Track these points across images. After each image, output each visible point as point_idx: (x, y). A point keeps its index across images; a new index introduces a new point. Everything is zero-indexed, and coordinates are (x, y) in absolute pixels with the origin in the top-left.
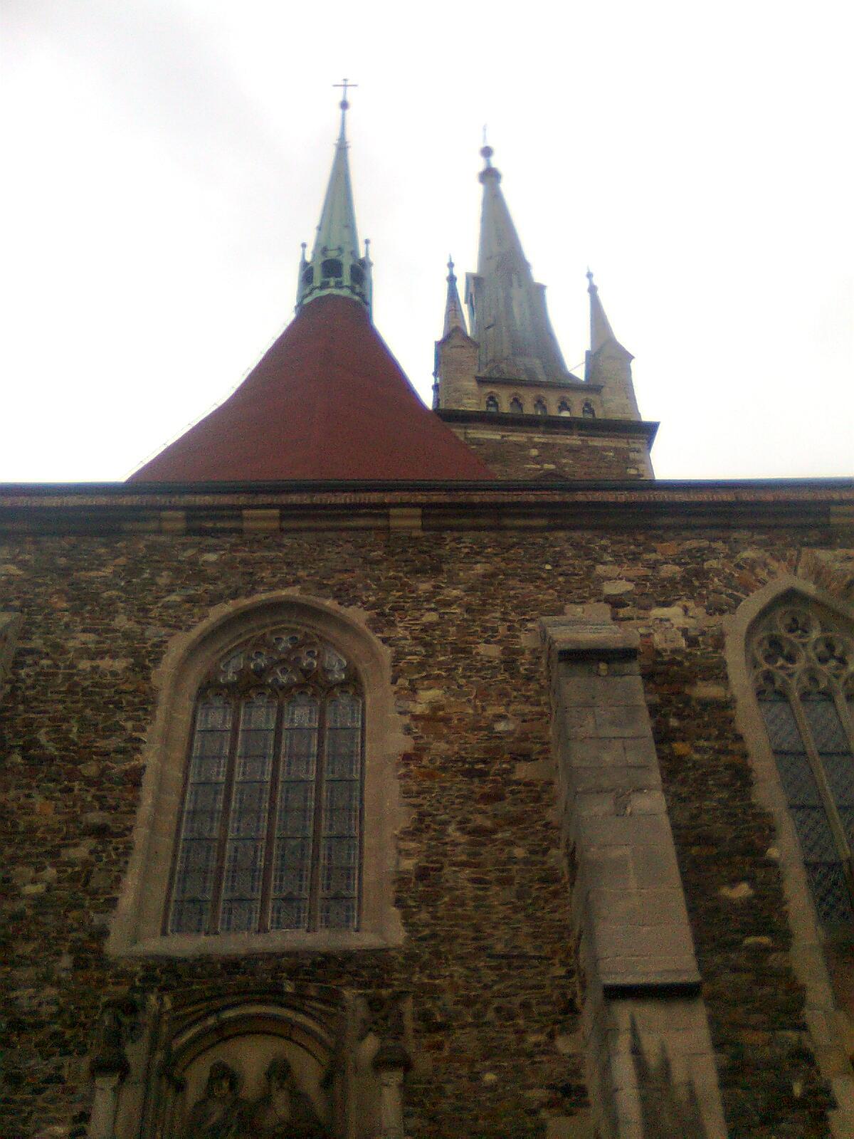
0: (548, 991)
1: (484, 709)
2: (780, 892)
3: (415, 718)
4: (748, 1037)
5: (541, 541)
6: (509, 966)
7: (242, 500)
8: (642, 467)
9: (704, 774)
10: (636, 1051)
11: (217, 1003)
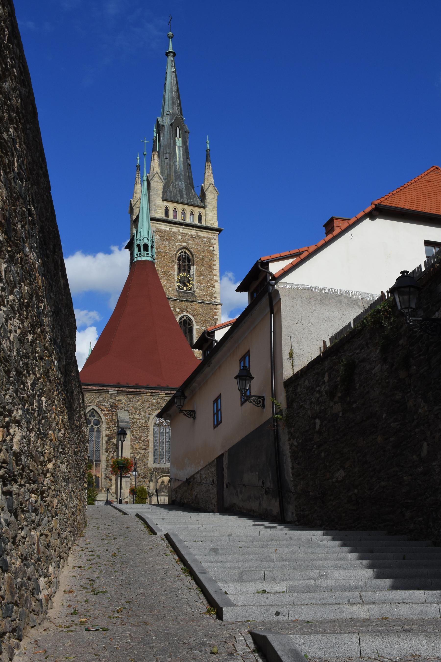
7: (160, 391)
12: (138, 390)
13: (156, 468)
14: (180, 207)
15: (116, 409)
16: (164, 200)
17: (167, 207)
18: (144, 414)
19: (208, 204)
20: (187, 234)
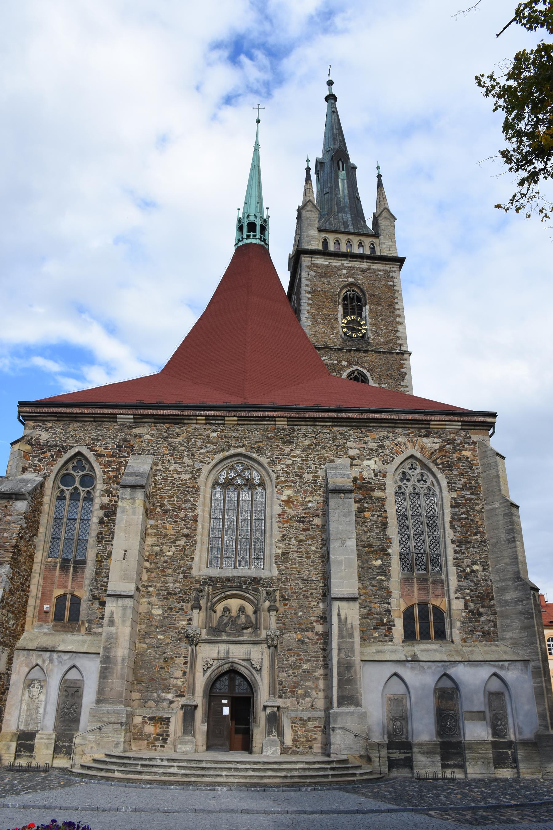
0: (318, 590)
1: (305, 498)
2: (390, 563)
3: (283, 501)
4: (374, 606)
5: (329, 431)
6: (308, 583)
7: (225, 413)
8: (395, 280)
9: (373, 524)
10: (339, 615)
11: (224, 590)
12: (177, 412)
13: (211, 578)
14: (343, 239)
15: (128, 453)
17: (325, 240)
18: (190, 461)
19: (382, 232)
20: (354, 268)
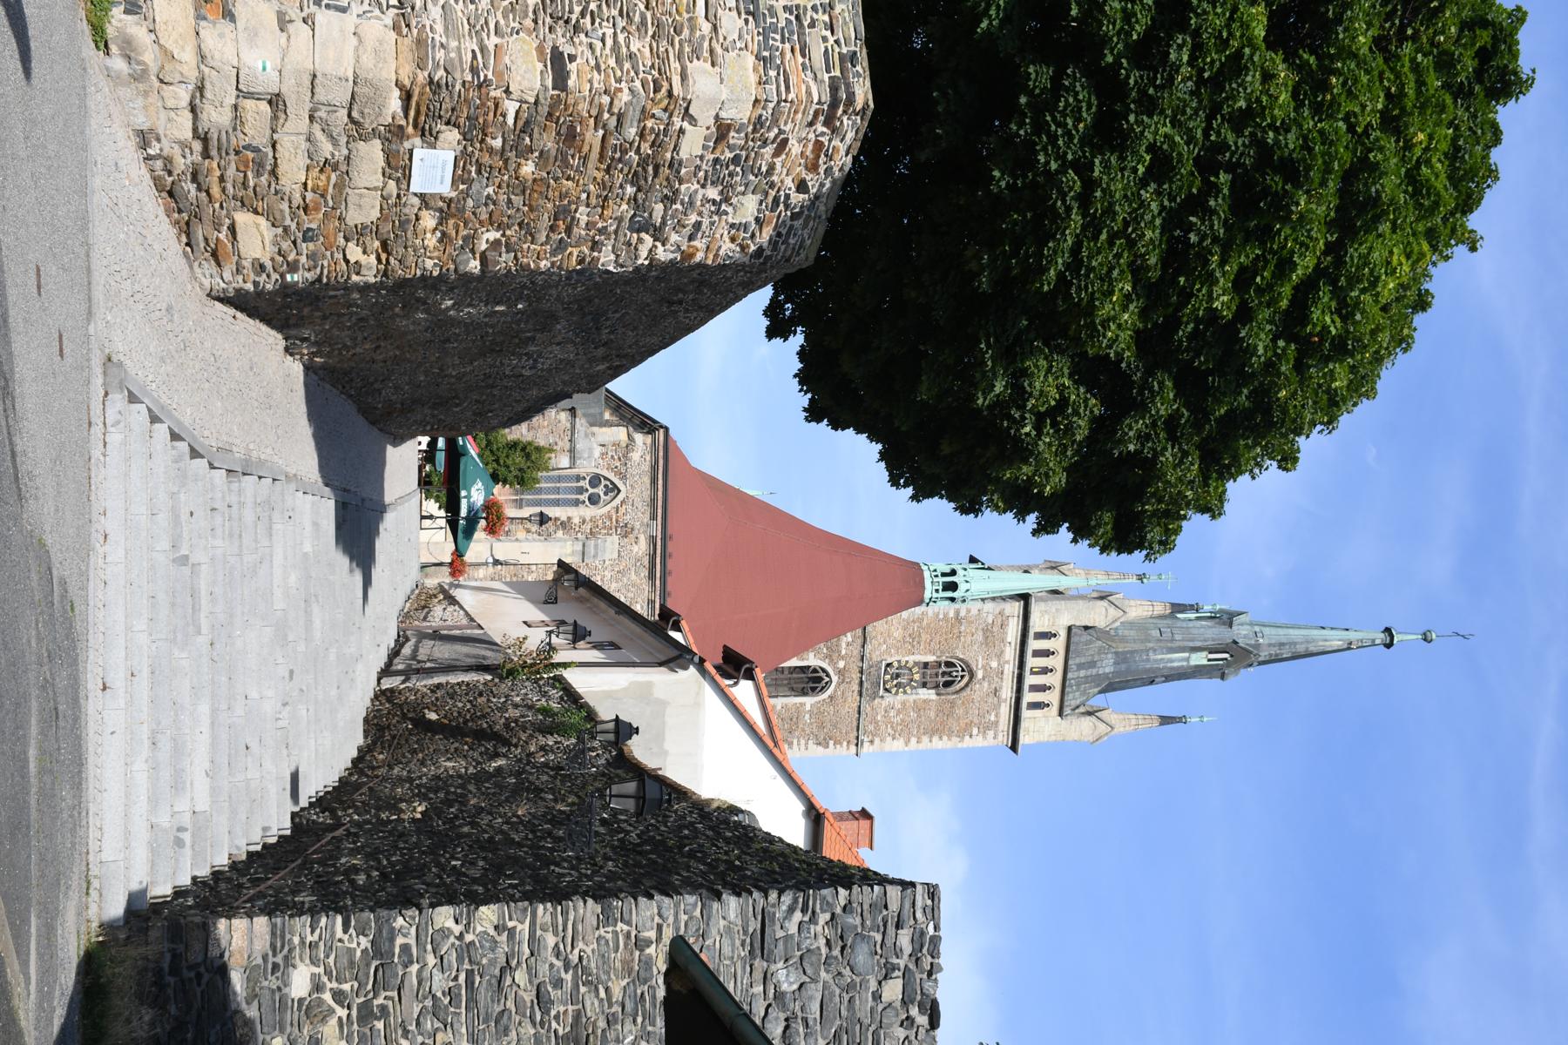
16: (1070, 629)
